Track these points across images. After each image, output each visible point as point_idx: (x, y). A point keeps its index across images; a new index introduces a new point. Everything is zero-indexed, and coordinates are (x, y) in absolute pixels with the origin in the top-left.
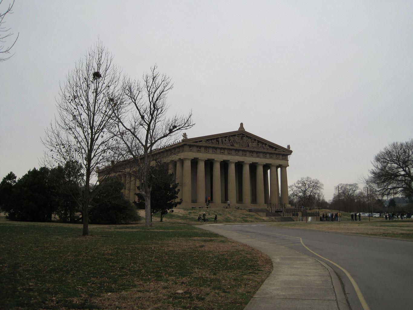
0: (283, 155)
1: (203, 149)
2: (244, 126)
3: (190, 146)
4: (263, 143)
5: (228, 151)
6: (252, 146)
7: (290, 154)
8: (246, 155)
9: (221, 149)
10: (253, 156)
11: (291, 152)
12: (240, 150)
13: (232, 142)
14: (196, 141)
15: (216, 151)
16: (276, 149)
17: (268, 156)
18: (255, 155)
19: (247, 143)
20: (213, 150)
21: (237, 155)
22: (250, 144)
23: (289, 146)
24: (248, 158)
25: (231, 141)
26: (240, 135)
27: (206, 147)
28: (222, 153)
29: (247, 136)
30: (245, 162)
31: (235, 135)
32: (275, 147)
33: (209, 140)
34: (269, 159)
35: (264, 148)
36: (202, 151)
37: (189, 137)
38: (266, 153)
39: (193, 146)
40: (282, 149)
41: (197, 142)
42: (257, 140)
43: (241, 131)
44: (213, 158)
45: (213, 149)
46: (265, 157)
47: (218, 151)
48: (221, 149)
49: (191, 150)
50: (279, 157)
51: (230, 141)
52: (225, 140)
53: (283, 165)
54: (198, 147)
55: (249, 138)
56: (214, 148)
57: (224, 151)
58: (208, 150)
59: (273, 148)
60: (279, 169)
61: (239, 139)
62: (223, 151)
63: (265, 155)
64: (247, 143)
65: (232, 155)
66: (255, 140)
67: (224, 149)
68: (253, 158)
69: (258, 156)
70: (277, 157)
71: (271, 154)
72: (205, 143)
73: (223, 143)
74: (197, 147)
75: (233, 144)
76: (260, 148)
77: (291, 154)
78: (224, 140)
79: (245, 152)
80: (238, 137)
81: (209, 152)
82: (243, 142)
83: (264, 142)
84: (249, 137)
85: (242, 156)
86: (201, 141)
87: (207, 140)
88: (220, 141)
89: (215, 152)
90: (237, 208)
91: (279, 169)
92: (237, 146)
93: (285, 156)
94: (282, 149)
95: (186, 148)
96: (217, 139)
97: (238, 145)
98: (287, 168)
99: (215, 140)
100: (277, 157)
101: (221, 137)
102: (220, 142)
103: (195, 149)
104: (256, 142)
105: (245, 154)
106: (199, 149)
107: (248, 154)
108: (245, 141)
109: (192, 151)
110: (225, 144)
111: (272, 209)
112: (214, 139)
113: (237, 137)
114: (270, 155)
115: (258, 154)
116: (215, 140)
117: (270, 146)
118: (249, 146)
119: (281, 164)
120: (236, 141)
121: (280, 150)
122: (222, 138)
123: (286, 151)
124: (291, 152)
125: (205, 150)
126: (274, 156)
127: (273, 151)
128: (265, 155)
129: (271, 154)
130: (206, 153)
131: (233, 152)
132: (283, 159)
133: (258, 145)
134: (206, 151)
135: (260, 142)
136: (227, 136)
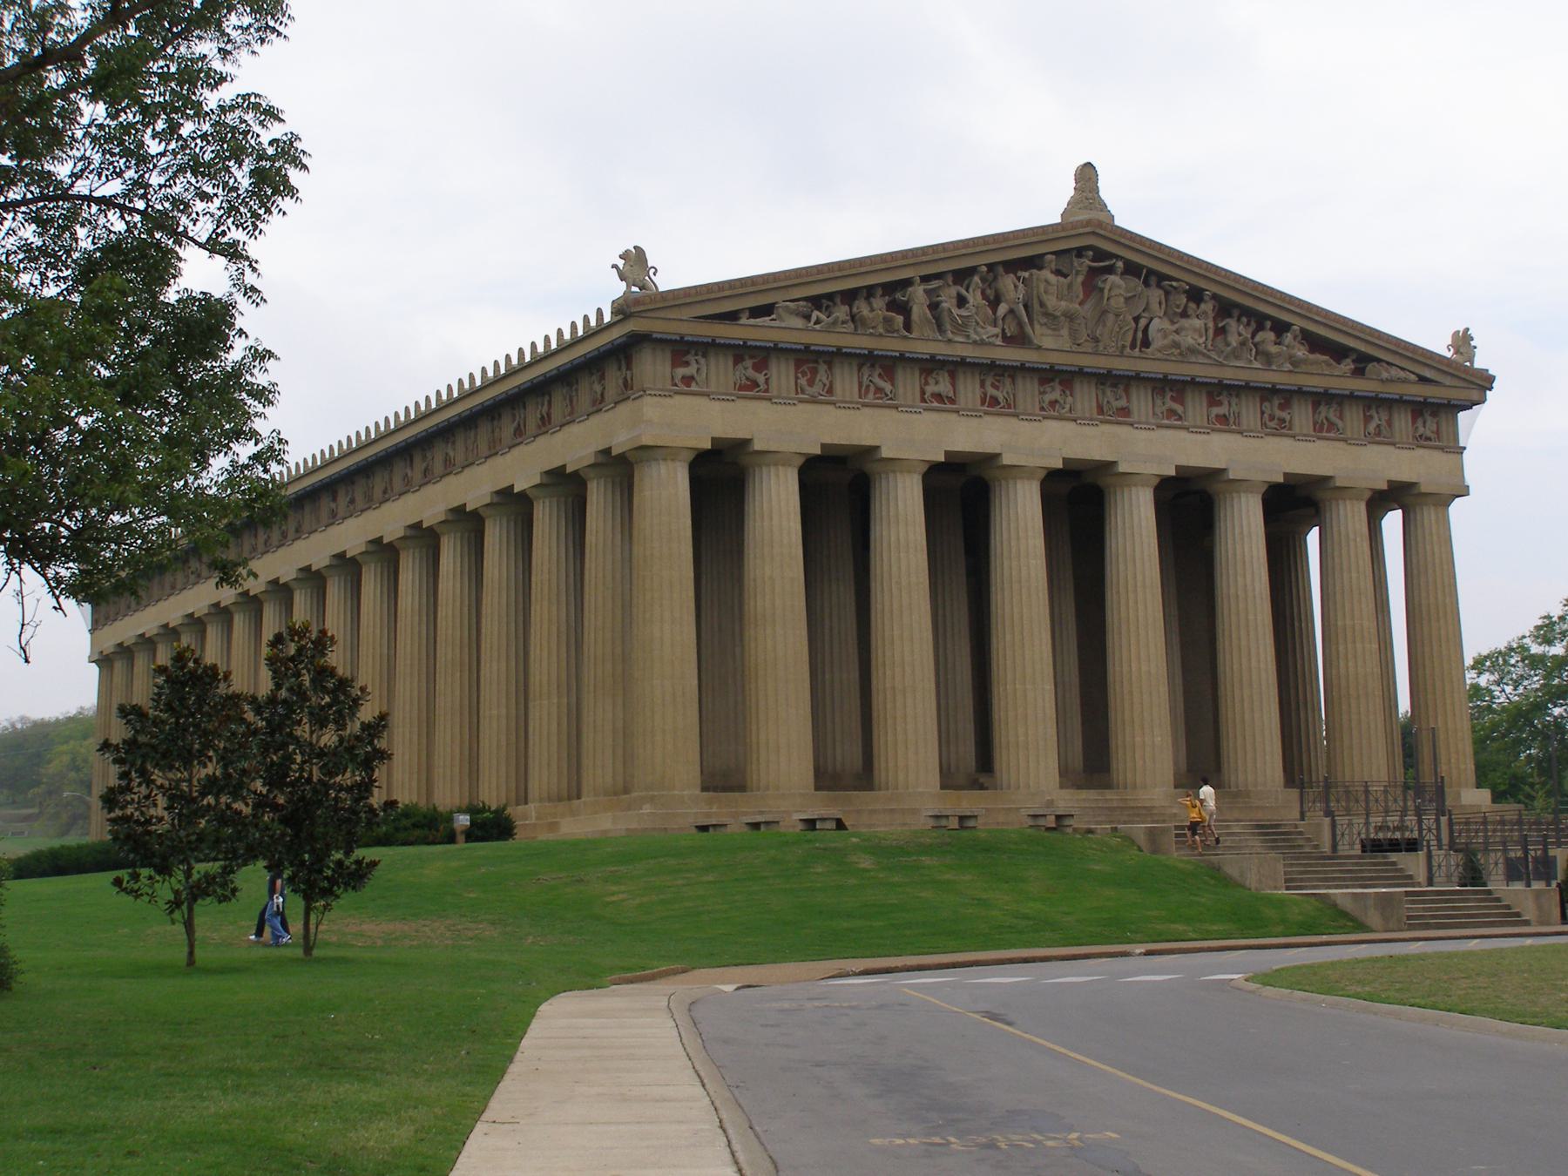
0: (1420, 409)
1: (782, 375)
2: (1108, 191)
3: (681, 349)
4: (1259, 320)
5: (983, 385)
6: (1176, 345)
7: (1475, 395)
8: (1125, 411)
10: (1180, 418)
11: (1482, 383)
12: (1081, 373)
13: (1011, 311)
15: (887, 387)
16: (1362, 363)
17: (1301, 416)
18: (1196, 408)
19: (1136, 319)
20: (865, 381)
21: (1052, 410)
22: (1156, 321)
23: (1463, 341)
24: (1144, 434)
25: (1003, 309)
26: (1076, 262)
27: (808, 359)
28: (938, 397)
29: (1132, 269)
30: (1122, 468)
31: (1033, 263)
32: (1352, 343)
33: (830, 296)
34: (1306, 438)
35: (1268, 358)
36: (774, 383)
37: (671, 276)
38: (1287, 396)
39: (707, 348)
40: (1405, 364)
41: (732, 316)
42: (1215, 297)
43: (1089, 223)
44: (868, 441)
45: (866, 371)
46: (1282, 428)
47: (908, 384)
48: (930, 366)
49: (688, 380)
50: (1390, 423)
51: (995, 303)
52: (961, 301)
53: (1423, 489)
54: (740, 352)
55: (1146, 284)
56: (868, 359)
57: (953, 385)
58: (822, 374)
59: (1338, 352)
60: (1392, 523)
61: (1070, 286)
62: (943, 385)
63: (1284, 415)
64: (1136, 319)
65: (1016, 415)
66: (1196, 295)
67: (955, 367)
68: (1183, 434)
69: (1223, 419)
70: (1372, 427)
71: (1328, 404)
72: (799, 323)
73: (940, 327)
74: (738, 360)
75: (1020, 325)
76: (1235, 355)
77: (1482, 401)
78: (947, 300)
79: (1120, 391)
80: (1058, 273)
81: (830, 391)
82: (1104, 312)
83: (1262, 308)
84: (1151, 272)
85: (1090, 421)
86: (766, 310)
87: (817, 302)
88: (919, 310)
89: (879, 390)
90: (1051, 821)
91: (1392, 523)
92: (1051, 346)
94: (1405, 364)
95: (652, 367)
96: (890, 288)
97: (1065, 332)
98: (1457, 508)
99: (879, 303)
100: (1372, 427)
101: (926, 279)
102: (915, 315)
103: (720, 371)
104: (1208, 307)
105: (1123, 403)
106: (751, 373)
107: (1141, 403)
108: (1118, 303)
109: (694, 388)
110: (961, 328)
111: (1334, 825)
112: (870, 291)
113: (1053, 278)
114: (1316, 406)
115: (1220, 404)
116: (879, 303)
117: (1315, 343)
118: (1146, 343)
119: (1404, 476)
120: (1042, 304)
121: (1394, 372)
122: (934, 284)
123: (1447, 381)
124: (1482, 383)
125: (803, 382)
126: (1353, 419)
127: (1339, 378)
128: (1282, 407)
129: (1322, 398)
130: (813, 401)
131: (1027, 393)
132: (1422, 441)
133: (1221, 331)
134: (811, 383)
135: (1236, 313)
136: (972, 271)
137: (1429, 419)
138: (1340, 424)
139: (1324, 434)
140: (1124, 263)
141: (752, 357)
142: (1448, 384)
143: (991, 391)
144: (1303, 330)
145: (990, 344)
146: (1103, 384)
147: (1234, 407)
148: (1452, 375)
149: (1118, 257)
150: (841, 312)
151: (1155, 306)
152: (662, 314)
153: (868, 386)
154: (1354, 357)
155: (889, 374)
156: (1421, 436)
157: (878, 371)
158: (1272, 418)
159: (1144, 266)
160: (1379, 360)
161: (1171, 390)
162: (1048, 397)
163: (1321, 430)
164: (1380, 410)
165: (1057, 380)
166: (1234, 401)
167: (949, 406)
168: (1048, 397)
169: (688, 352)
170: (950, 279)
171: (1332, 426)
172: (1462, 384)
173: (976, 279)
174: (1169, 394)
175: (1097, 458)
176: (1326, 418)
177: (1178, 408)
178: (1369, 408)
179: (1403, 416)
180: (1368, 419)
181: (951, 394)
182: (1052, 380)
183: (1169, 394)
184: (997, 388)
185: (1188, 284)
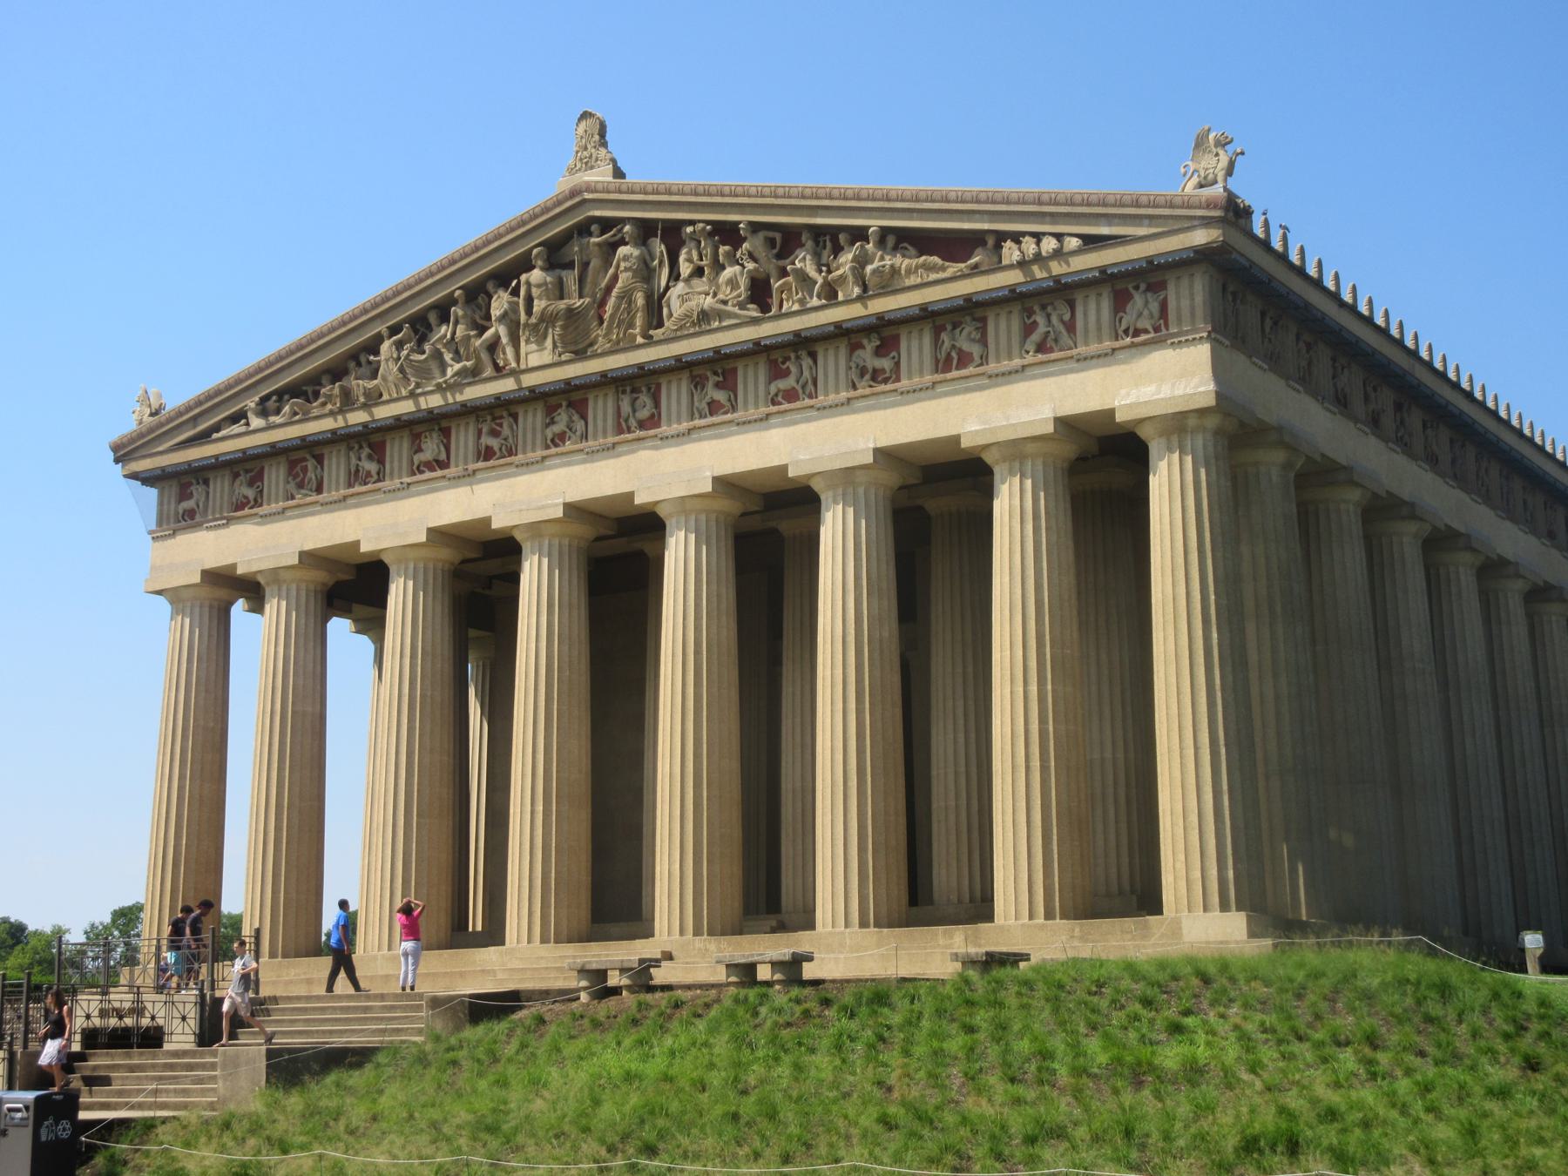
4: (828, 240)
5: (480, 433)
9: (416, 438)
15: (372, 467)
29: (646, 230)
38: (885, 332)
42: (755, 227)
43: (574, 193)
63: (885, 364)
66: (727, 234)
67: (438, 423)
79: (644, 398)
93: (1157, 287)
101: (394, 330)
109: (198, 518)
114: (937, 331)
115: (787, 373)
128: (879, 352)
129: (931, 318)
136: (450, 301)
139: (955, 374)
140: (633, 225)
141: (247, 471)
144: (885, 232)
146: (624, 392)
147: (806, 373)
149: (623, 221)
150: (332, 390)
151: (685, 269)
152: (144, 452)
153: (357, 471)
154: (991, 242)
155: (378, 454)
156: (1126, 332)
157: (366, 451)
158: (862, 372)
160: (1016, 237)
161: (716, 373)
162: (549, 433)
163: (947, 367)
165: (564, 404)
166: (807, 362)
167: (439, 473)
168: (549, 433)
169: (190, 484)
170: (432, 318)
171: (964, 360)
173: (457, 311)
174: (710, 385)
175: (610, 492)
176: (953, 347)
177: (720, 396)
178: (1030, 312)
180: (1028, 330)
181: (443, 456)
182: (560, 406)
183: (713, 379)
184: (494, 433)
185: (708, 222)
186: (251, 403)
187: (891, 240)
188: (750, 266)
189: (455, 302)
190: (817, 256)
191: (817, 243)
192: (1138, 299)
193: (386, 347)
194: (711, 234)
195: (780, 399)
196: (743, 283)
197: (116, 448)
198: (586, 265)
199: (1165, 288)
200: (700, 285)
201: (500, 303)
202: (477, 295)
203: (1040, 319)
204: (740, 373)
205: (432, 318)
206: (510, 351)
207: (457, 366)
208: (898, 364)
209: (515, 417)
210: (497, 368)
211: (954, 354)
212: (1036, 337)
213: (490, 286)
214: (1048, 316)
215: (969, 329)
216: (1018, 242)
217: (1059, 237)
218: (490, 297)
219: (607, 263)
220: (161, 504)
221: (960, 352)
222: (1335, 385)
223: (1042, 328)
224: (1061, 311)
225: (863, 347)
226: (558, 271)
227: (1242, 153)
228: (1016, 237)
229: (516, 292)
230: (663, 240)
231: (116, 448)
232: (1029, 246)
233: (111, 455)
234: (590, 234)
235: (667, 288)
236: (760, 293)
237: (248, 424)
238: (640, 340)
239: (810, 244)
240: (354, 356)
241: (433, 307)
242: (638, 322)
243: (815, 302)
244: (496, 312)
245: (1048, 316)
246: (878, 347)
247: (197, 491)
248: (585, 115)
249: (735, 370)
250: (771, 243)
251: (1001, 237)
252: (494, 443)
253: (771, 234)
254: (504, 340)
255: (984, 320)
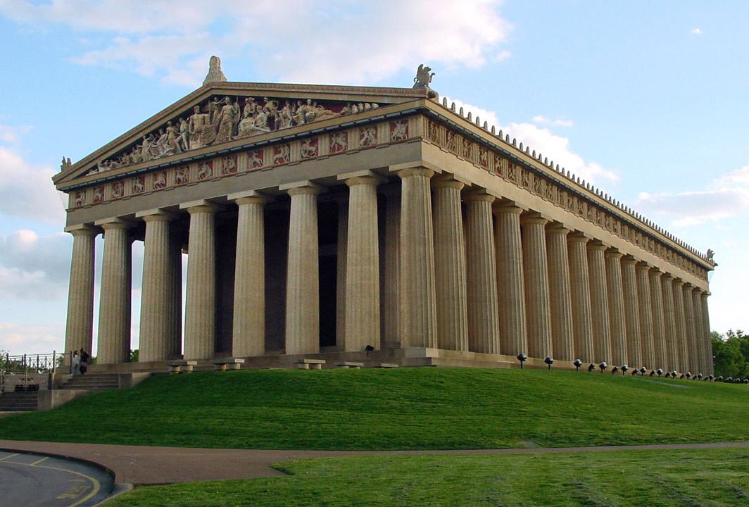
4: (293, 102)
5: (176, 173)
9: (155, 175)
14: (82, 171)
28: (158, 185)
29: (233, 99)
33: (121, 153)
41: (83, 175)
42: (270, 99)
43: (208, 85)
50: (376, 136)
63: (313, 149)
66: (260, 101)
79: (232, 161)
87: (114, 158)
101: (147, 136)
104: (270, 105)
109: (82, 205)
115: (280, 152)
123: (399, 101)
129: (330, 132)
137: (399, 126)
138: (343, 144)
142: (398, 103)
143: (179, 176)
144: (313, 101)
145: (167, 156)
148: (401, 97)
149: (225, 96)
151: (246, 114)
152: (65, 180)
157: (138, 180)
159: (236, 96)
160: (357, 103)
164: (369, 130)
166: (287, 148)
172: (408, 100)
176: (336, 143)
177: (257, 160)
178: (362, 131)
179: (383, 127)
181: (164, 182)
184: (182, 174)
185: (253, 97)
186: (99, 162)
187: (315, 104)
188: (268, 113)
189: (168, 126)
190: (290, 108)
191: (291, 104)
192: (399, 126)
193: (145, 142)
194: (254, 101)
195: (277, 162)
196: (265, 119)
197: (53, 179)
198: (213, 112)
199: (408, 123)
200: (250, 120)
201: (183, 126)
202: (175, 122)
203: (365, 133)
204: (264, 152)
205: (161, 132)
206: (186, 143)
207: (168, 149)
208: (317, 149)
209: (188, 168)
210: (182, 150)
211: (336, 145)
212: (364, 140)
213: (180, 120)
214: (368, 132)
215: (342, 135)
216: (358, 106)
217: (371, 103)
218: (180, 124)
219: (220, 111)
220: (70, 200)
221: (338, 144)
222: (480, 158)
223: (366, 136)
224: (372, 131)
225: (305, 143)
226: (203, 115)
227: (433, 74)
228: (357, 103)
229: (188, 122)
230: (238, 103)
231: (53, 179)
232: (361, 106)
233: (52, 182)
234: (214, 101)
235: (240, 121)
236: (271, 122)
237: (98, 170)
238: (230, 140)
239: (288, 105)
240: (134, 145)
241: (160, 127)
242: (230, 132)
243: (289, 126)
244: (182, 130)
245: (368, 132)
246: (310, 143)
247: (82, 195)
248: (213, 57)
249: (262, 151)
250: (275, 104)
251: (353, 103)
252: (181, 177)
253: (275, 101)
254: (184, 140)
255: (347, 133)
